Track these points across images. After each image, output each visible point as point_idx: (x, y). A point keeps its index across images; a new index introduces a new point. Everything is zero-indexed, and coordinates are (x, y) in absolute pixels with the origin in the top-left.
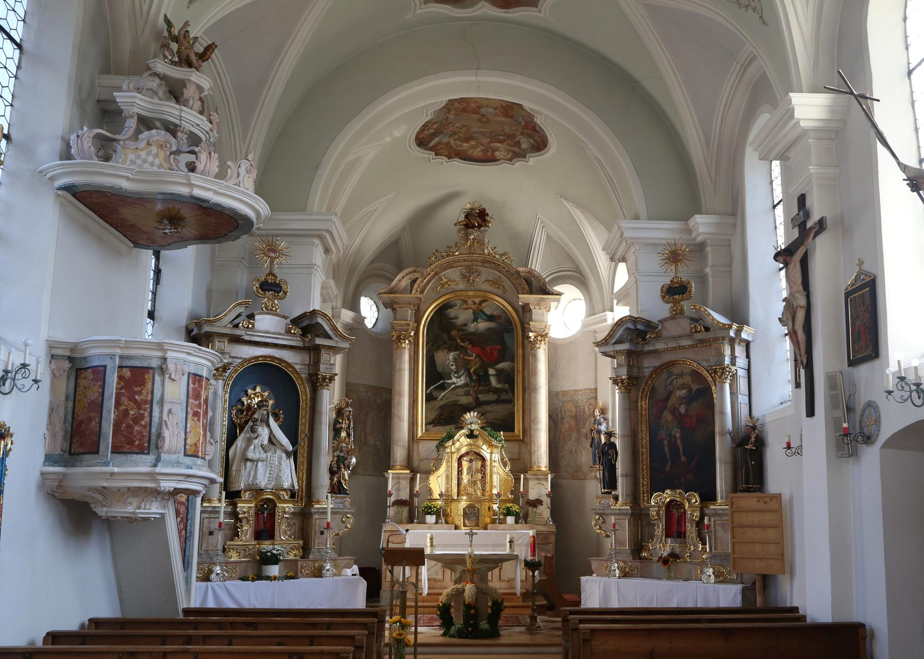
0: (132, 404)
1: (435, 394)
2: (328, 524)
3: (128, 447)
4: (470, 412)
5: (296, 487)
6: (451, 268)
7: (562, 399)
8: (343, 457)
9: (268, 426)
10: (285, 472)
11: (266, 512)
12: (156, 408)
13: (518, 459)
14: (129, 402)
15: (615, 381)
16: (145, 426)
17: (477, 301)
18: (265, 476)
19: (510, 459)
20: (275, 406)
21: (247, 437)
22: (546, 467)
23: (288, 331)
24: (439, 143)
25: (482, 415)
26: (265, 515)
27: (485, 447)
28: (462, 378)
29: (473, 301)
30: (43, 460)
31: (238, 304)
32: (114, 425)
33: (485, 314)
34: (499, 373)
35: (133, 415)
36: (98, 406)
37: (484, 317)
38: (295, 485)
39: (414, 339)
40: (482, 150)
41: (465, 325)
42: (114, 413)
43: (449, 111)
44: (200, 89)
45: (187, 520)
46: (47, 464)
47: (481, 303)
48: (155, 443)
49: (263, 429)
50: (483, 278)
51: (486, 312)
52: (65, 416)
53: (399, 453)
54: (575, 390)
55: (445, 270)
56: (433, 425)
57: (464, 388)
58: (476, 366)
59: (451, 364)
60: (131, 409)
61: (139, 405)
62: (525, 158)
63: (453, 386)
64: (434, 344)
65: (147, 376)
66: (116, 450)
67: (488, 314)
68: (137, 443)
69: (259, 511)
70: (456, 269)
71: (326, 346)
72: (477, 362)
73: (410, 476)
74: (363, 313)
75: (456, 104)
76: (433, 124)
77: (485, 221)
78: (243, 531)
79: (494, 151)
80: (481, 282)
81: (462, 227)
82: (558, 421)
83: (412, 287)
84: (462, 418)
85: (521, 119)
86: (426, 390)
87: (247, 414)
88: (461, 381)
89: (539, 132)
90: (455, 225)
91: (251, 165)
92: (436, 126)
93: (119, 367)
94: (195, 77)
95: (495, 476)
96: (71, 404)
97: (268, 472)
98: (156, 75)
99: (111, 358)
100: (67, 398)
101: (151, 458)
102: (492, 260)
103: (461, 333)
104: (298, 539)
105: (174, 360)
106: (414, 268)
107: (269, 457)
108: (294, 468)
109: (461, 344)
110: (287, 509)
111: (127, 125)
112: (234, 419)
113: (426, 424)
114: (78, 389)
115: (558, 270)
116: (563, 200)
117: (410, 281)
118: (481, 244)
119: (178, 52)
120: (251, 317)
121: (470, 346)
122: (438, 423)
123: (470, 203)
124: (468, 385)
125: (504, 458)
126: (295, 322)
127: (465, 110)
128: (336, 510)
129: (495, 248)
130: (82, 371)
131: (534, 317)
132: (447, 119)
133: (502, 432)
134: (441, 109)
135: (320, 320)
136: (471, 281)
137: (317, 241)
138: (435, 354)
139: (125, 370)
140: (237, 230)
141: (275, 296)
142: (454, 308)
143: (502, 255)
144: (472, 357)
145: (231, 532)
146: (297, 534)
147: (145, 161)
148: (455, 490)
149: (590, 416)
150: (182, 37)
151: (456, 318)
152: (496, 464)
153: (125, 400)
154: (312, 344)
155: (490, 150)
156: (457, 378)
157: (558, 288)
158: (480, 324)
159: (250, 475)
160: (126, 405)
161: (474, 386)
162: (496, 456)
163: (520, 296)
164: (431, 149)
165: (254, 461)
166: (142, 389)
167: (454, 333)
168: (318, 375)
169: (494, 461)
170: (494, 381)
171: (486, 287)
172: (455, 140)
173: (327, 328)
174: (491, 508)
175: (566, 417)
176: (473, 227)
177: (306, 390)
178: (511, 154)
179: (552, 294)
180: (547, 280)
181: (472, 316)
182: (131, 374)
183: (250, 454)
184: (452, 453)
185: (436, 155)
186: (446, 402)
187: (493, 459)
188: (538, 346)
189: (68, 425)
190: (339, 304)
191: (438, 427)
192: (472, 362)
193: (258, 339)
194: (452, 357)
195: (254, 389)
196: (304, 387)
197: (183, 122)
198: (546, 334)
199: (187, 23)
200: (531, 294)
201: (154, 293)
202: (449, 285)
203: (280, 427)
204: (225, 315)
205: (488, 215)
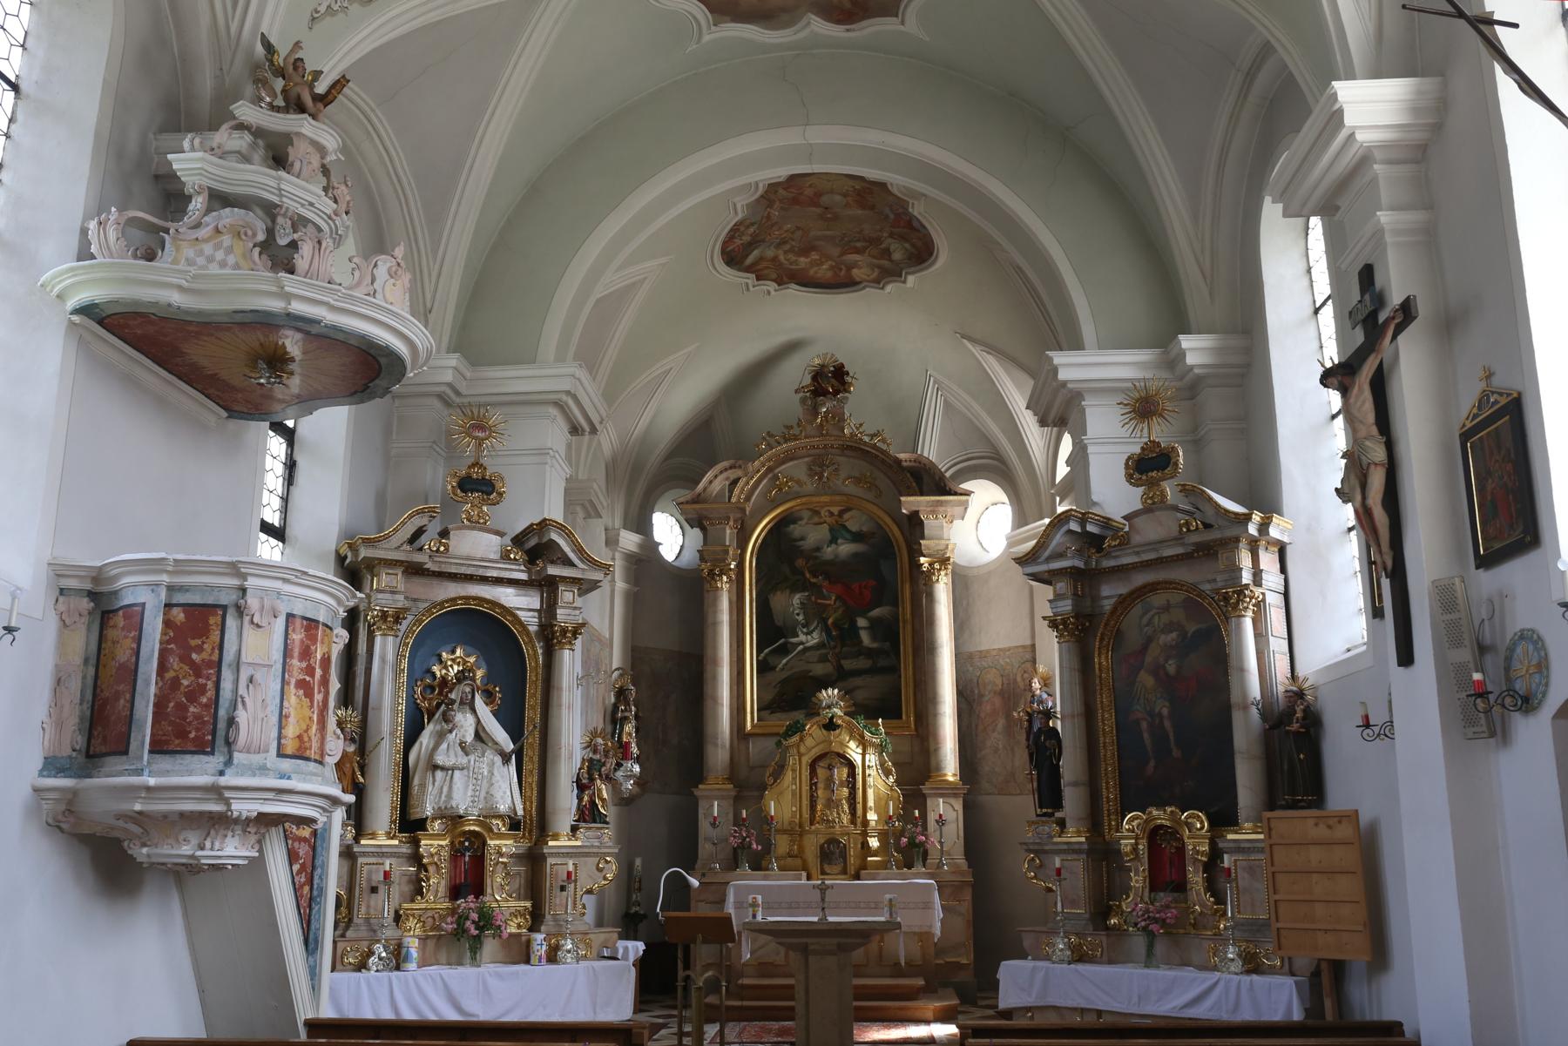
0: (186, 668)
1: (771, 660)
2: (569, 874)
3: (177, 742)
4: (826, 690)
5: (520, 812)
6: (792, 459)
7: (979, 664)
8: (599, 761)
9: (473, 711)
10: (500, 787)
11: (468, 854)
12: (227, 675)
14: (181, 665)
15: (1053, 624)
16: (207, 706)
17: (835, 510)
18: (465, 793)
19: (894, 764)
20: (489, 678)
21: (437, 732)
22: (955, 775)
23: (505, 556)
24: (761, 259)
25: (846, 693)
26: (467, 859)
27: (852, 744)
28: (815, 635)
30: (40, 766)
31: (418, 512)
32: (156, 705)
33: (849, 531)
34: (875, 625)
35: (188, 686)
36: (130, 673)
37: (848, 536)
38: (517, 808)
39: (737, 576)
40: (832, 268)
41: (818, 549)
42: (156, 683)
43: (770, 204)
44: (321, 150)
45: (314, 868)
46: (45, 773)
47: (841, 513)
48: (224, 734)
49: (465, 717)
50: (843, 474)
52: (81, 691)
53: (719, 753)
54: (1000, 650)
55: (783, 463)
56: (769, 712)
57: (818, 649)
60: (184, 677)
61: (197, 670)
62: (901, 276)
63: (801, 647)
64: (768, 582)
65: (212, 621)
66: (158, 748)
68: (192, 735)
69: (456, 853)
70: (800, 461)
71: (565, 578)
72: (838, 608)
73: (733, 793)
74: (657, 536)
75: (781, 191)
76: (748, 227)
77: (844, 383)
78: (430, 886)
79: (849, 269)
81: (808, 394)
82: (974, 700)
83: (731, 492)
84: (813, 699)
85: (887, 211)
86: (757, 657)
87: (440, 693)
88: (814, 639)
89: (918, 231)
90: (797, 391)
91: (399, 264)
92: (752, 230)
93: (166, 605)
94: (304, 126)
95: (870, 793)
96: (91, 671)
97: (471, 787)
98: (241, 127)
99: (153, 591)
100: (86, 661)
101: (216, 761)
102: (857, 445)
104: (525, 899)
105: (259, 592)
106: (732, 462)
107: (472, 762)
108: (515, 779)
110: (504, 850)
111: (191, 207)
112: (418, 701)
114: (103, 646)
115: (965, 457)
116: (965, 341)
117: (727, 483)
118: (839, 421)
119: (284, 91)
120: (444, 534)
121: (826, 583)
123: (818, 356)
125: (886, 762)
126: (518, 541)
127: (795, 201)
128: (587, 850)
129: (861, 425)
130: (111, 615)
131: (926, 532)
132: (768, 217)
133: (880, 720)
134: (757, 201)
135: (554, 536)
136: (825, 480)
137: (553, 411)
138: (771, 597)
139: (175, 611)
140: (382, 375)
141: (483, 500)
142: (800, 522)
143: (872, 436)
144: (831, 599)
145: (412, 887)
146: (522, 891)
147: (210, 259)
148: (806, 815)
149: (1025, 690)
150: (291, 67)
151: (802, 539)
152: (873, 772)
153: (174, 661)
154: (543, 575)
155: (843, 267)
156: (807, 634)
157: (966, 486)
158: (842, 548)
159: (441, 793)
160: (175, 671)
161: (835, 647)
162: (872, 759)
163: (903, 499)
164: (748, 270)
165: (448, 770)
166: (203, 643)
167: (800, 562)
168: (552, 626)
169: (869, 766)
170: (865, 638)
171: (850, 488)
172: (785, 252)
173: (567, 549)
175: (987, 693)
176: (825, 393)
177: (535, 652)
178: (877, 272)
179: (956, 494)
180: (948, 475)
181: (828, 536)
182: (186, 617)
183: (440, 759)
185: (758, 279)
186: (789, 673)
187: (867, 763)
188: (934, 578)
189: (86, 706)
190: (618, 522)
191: (778, 715)
193: (453, 570)
195: (453, 652)
196: (533, 647)
197: (284, 199)
198: (948, 559)
199: (297, 45)
200: (922, 494)
201: (285, 499)
202: (789, 487)
203: (495, 714)
204: (396, 530)
205: (848, 374)
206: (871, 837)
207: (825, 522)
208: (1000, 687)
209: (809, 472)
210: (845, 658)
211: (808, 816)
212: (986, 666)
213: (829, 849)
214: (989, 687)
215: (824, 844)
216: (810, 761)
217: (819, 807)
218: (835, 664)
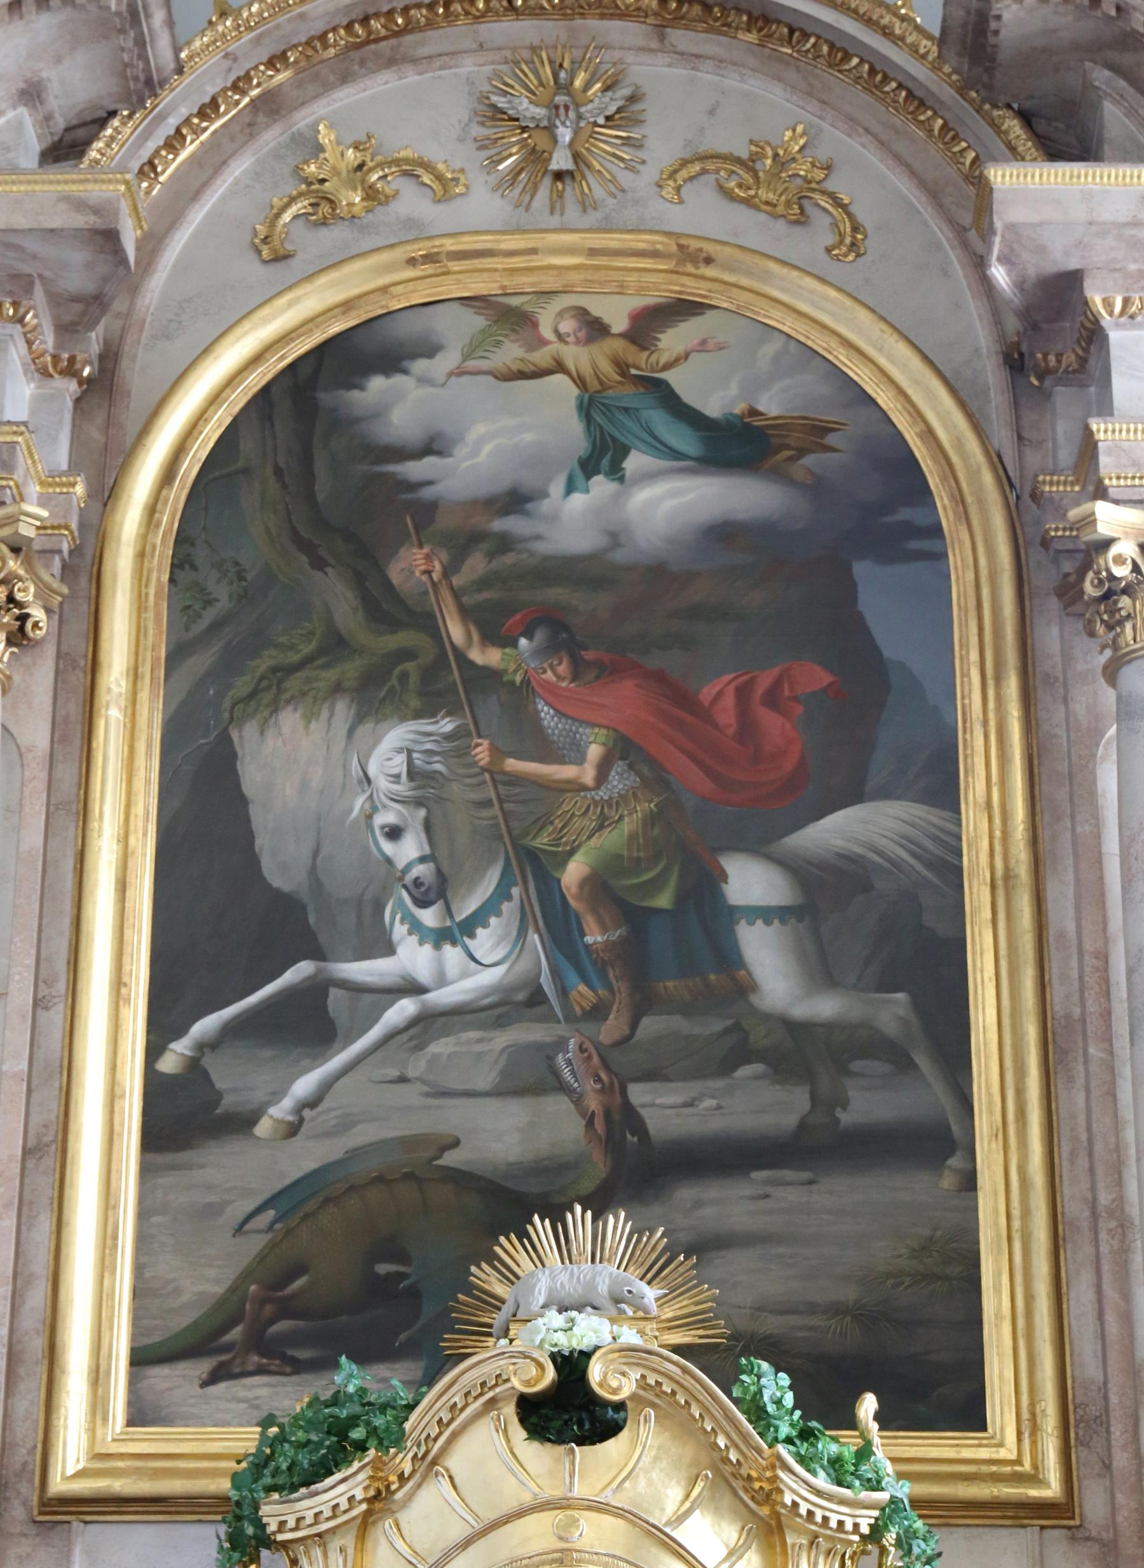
28: (484, 942)
29: (582, 314)
37: (684, 439)
51: (689, 396)
56: (204, 1366)
58: (613, 839)
59: (386, 817)
67: (713, 407)
72: (623, 799)
80: (650, 174)
86: (153, 1052)
103: (476, 565)
109: (476, 656)
113: (140, 1359)
122: (258, 1342)
124: (537, 998)
142: (420, 366)
144: (580, 760)
151: (432, 447)
156: (442, 937)
158: (642, 496)
161: (598, 1012)
186: (331, 1150)
192: (570, 804)
194: (399, 764)
207: (559, 367)
209: (477, 131)
210: (650, 1075)
218: (593, 1104)
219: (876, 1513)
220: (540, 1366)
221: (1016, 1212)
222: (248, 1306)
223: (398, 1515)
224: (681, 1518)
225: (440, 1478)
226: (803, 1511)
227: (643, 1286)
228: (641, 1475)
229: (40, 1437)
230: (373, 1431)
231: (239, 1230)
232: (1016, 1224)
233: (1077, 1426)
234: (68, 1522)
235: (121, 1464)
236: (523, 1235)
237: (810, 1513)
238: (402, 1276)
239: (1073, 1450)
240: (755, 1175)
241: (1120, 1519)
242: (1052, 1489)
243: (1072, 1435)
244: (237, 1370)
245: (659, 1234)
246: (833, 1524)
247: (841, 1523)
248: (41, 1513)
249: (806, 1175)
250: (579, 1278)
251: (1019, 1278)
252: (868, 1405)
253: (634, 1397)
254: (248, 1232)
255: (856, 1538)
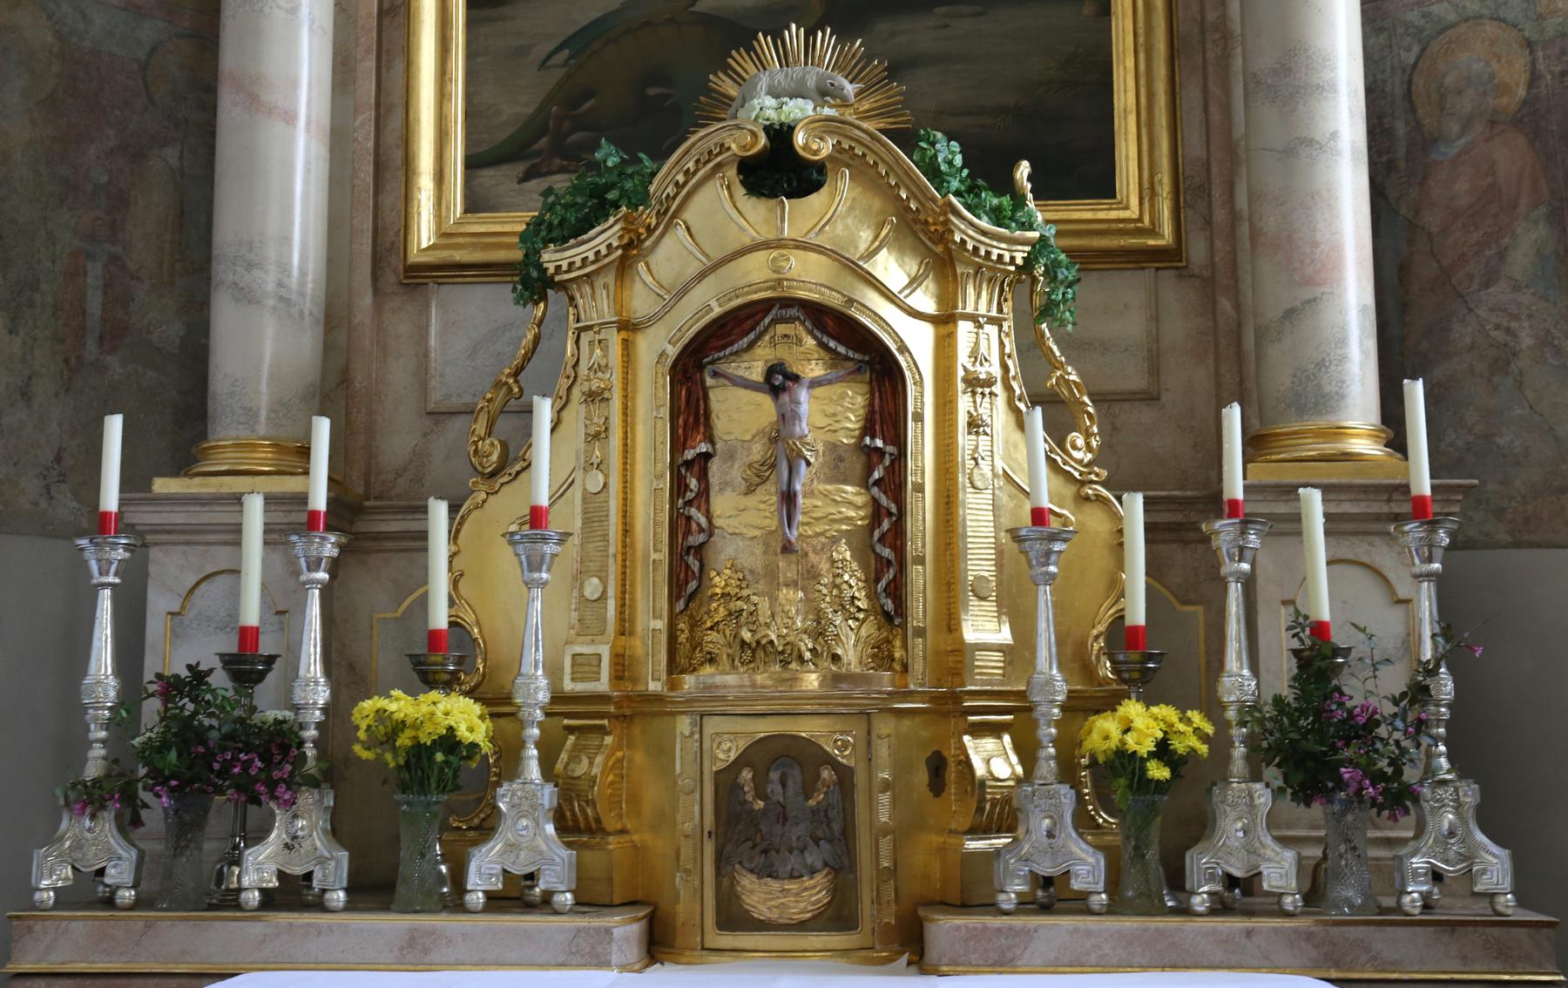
7: (1413, 16)
13: (1149, 397)
27: (891, 268)
56: (520, 168)
125: (1054, 365)
148: (652, 622)
152: (997, 413)
169: (973, 383)
174: (951, 774)
184: (629, 326)
187: (963, 357)
206: (979, 730)
208: (1522, 92)
211: (660, 624)
212: (1452, 17)
213: (760, 794)
214: (1467, 104)
215: (737, 765)
216: (673, 352)
217: (718, 582)
219: (1028, 248)
220: (754, 134)
221: (1141, 31)
222: (551, 122)
223: (648, 259)
224: (871, 254)
225: (678, 227)
226: (970, 247)
227: (846, 83)
228: (839, 220)
229: (403, 223)
230: (624, 194)
231: (543, 65)
232: (1141, 40)
233: (1185, 193)
234: (426, 284)
235: (461, 240)
236: (750, 49)
237: (976, 249)
238: (668, 96)
239: (1182, 210)
240: (936, 10)
241: (1217, 259)
242: (1166, 236)
243: (1182, 199)
244: (544, 170)
245: (858, 43)
246: (994, 257)
247: (1000, 257)
248: (406, 277)
249: (978, 9)
250: (792, 77)
251: (1142, 82)
252: (1024, 170)
253: (830, 157)
254: (549, 67)
255: (1012, 268)
